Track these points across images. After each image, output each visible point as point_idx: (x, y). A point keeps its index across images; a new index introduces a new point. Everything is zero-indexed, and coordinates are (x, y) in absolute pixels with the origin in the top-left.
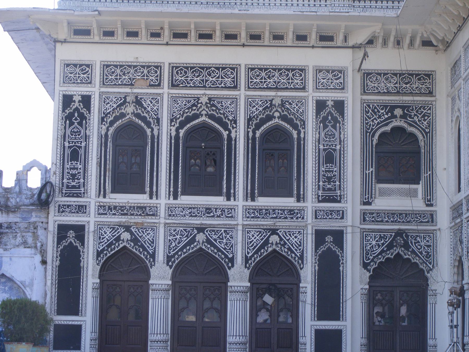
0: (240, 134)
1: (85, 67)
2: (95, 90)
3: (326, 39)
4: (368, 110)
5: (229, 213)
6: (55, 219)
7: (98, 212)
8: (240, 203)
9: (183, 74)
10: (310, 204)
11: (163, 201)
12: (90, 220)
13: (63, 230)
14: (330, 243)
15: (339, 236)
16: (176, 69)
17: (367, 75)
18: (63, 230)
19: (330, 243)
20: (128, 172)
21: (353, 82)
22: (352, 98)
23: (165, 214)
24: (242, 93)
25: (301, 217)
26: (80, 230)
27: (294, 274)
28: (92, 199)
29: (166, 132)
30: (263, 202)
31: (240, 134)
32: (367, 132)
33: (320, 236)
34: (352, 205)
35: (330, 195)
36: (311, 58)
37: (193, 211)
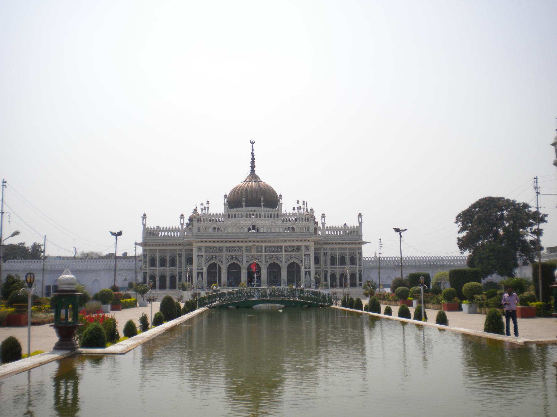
0: (168, 259)
1: (146, 250)
2: (148, 253)
3: (180, 245)
4: (186, 255)
5: (166, 270)
6: (143, 271)
7: (149, 270)
8: (168, 268)
9: (160, 250)
10: (178, 268)
11: (157, 268)
12: (148, 271)
13: (144, 273)
14: (180, 273)
15: (181, 272)
16: (159, 250)
17: (186, 250)
18: (144, 273)
19: (180, 273)
20: (153, 263)
21: (183, 251)
22: (183, 253)
23: (158, 270)
24: (168, 253)
25: (176, 270)
26: (146, 273)
27: (176, 278)
28: (148, 268)
29: (158, 259)
30: (171, 268)
31: (168, 259)
32: (186, 258)
33: (179, 272)
34: (183, 268)
35: (180, 267)
36: (178, 248)
37: (162, 269)
